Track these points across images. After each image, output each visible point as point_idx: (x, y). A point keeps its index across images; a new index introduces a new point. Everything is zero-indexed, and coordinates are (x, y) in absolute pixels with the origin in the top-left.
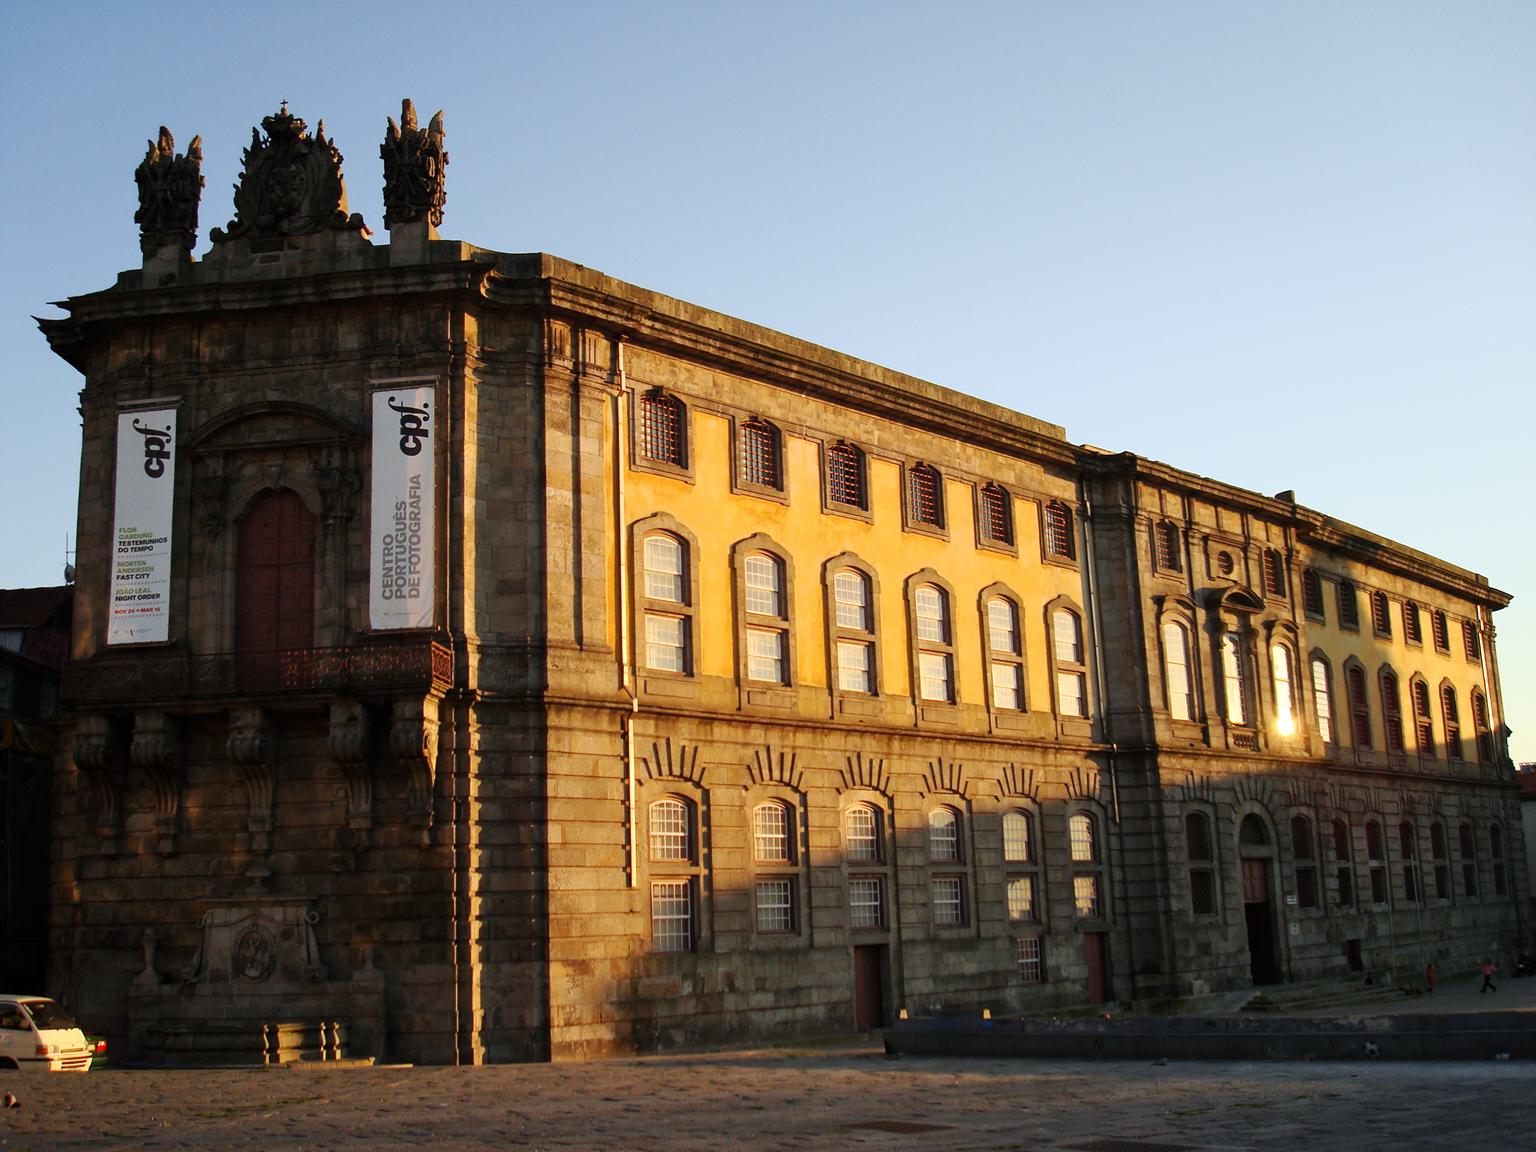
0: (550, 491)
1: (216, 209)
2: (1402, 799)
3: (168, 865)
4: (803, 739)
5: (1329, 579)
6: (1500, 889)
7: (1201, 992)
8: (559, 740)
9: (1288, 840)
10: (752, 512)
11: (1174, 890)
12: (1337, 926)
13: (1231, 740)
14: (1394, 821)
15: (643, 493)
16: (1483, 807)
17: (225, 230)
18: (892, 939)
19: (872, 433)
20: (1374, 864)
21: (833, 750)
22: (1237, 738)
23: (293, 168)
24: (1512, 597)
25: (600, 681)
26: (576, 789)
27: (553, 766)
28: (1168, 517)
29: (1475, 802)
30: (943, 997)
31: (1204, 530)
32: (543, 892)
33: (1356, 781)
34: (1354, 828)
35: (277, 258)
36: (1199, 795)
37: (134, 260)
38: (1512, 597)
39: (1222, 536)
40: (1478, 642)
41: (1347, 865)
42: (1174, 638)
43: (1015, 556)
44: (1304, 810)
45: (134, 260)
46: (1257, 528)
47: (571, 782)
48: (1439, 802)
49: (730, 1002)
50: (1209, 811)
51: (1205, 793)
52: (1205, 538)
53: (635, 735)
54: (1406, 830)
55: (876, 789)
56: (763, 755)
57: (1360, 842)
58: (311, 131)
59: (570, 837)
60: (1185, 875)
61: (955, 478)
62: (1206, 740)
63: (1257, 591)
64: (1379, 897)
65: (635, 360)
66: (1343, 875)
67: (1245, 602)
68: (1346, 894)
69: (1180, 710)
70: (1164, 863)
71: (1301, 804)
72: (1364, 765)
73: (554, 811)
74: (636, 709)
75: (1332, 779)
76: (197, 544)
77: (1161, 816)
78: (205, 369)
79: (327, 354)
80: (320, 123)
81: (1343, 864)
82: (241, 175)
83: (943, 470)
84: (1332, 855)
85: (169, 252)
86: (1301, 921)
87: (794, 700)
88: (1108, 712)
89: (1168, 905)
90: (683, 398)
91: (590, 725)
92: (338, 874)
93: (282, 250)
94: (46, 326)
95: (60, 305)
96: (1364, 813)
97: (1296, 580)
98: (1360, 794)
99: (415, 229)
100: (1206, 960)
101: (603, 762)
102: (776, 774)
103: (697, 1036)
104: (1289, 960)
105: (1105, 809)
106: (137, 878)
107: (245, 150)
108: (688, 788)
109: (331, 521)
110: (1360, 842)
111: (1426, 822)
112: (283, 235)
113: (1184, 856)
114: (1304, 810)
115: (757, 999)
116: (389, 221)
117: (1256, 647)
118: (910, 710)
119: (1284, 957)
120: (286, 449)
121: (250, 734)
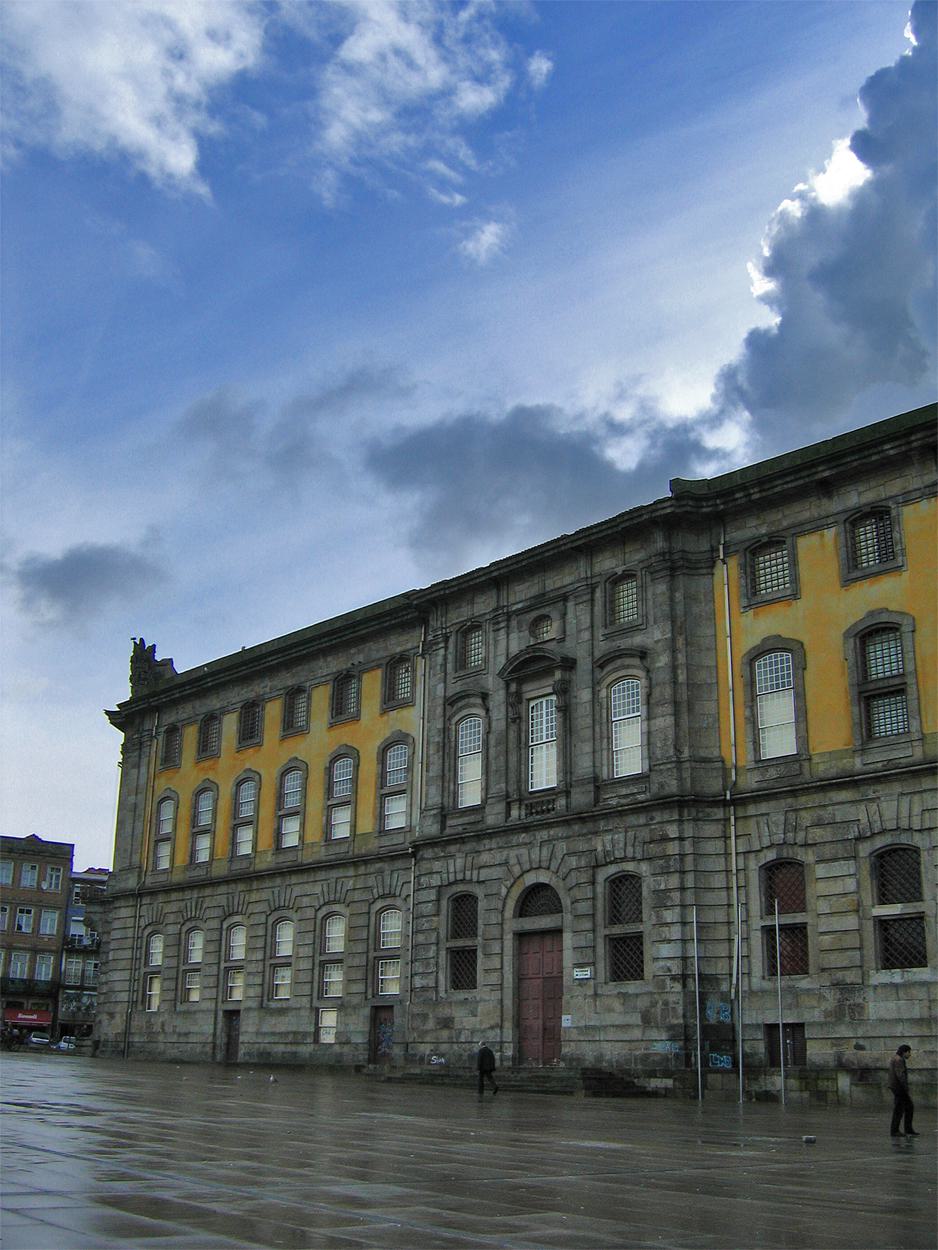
12: (666, 1003)
31: (514, 609)
36: (460, 877)
44: (630, 867)
51: (468, 873)
52: (519, 612)
56: (189, 904)
71: (615, 861)
96: (860, 838)
100: (445, 1034)
102: (193, 913)
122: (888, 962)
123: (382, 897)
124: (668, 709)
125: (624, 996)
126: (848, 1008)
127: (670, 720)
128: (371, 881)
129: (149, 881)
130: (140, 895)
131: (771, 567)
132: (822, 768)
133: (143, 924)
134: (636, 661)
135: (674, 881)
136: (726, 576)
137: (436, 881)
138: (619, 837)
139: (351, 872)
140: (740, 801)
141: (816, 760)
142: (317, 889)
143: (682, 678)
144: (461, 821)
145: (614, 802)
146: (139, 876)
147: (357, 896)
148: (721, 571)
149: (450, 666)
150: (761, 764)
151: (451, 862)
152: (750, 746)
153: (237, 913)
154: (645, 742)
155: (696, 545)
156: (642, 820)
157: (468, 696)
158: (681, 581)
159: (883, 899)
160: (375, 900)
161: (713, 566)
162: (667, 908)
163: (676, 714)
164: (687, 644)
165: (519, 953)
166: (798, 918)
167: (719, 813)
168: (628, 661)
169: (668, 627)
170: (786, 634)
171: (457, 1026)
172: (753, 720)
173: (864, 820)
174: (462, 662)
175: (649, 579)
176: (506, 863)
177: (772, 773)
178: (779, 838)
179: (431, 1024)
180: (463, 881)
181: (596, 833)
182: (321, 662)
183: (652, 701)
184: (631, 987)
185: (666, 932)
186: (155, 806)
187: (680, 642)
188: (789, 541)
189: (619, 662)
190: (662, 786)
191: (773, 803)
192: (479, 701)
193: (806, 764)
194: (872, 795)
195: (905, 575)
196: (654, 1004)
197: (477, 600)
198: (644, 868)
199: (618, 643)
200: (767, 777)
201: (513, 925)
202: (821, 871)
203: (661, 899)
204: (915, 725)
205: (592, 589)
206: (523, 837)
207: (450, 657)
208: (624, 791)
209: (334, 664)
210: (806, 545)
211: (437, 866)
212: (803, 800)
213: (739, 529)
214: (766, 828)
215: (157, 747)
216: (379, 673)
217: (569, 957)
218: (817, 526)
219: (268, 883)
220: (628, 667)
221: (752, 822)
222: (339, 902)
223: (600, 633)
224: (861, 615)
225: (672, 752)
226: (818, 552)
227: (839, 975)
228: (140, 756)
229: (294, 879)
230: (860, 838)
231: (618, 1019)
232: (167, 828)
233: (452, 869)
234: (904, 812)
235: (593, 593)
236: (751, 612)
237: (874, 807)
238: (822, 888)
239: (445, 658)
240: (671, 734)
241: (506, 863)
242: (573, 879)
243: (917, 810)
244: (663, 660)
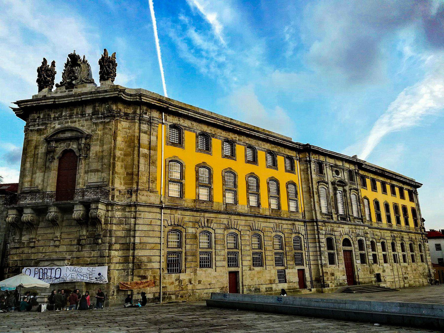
0: (141, 149)
1: (58, 79)
2: (392, 236)
3: (33, 250)
5: (368, 178)
6: (422, 261)
7: (332, 286)
8: (140, 215)
9: (357, 246)
11: (323, 258)
13: (339, 219)
14: (391, 241)
16: (416, 239)
17: (59, 84)
18: (240, 270)
19: (236, 138)
20: (384, 253)
21: (224, 219)
22: (341, 218)
23: (76, 67)
24: (422, 185)
25: (154, 199)
26: (146, 228)
27: (139, 221)
28: (321, 161)
29: (414, 237)
30: (255, 286)
31: (331, 164)
32: (134, 256)
33: (378, 231)
34: (377, 243)
35: (72, 91)
37: (36, 93)
38: (422, 185)
39: (336, 166)
40: (413, 196)
41: (376, 253)
42: (323, 192)
43: (277, 169)
44: (362, 238)
45: (36, 93)
46: (347, 165)
47: (143, 226)
48: (403, 237)
49: (190, 287)
50: (333, 237)
52: (332, 166)
53: (164, 213)
54: (393, 245)
55: (236, 229)
56: (202, 219)
57: (379, 246)
58: (82, 58)
59: (142, 241)
60: (326, 253)
61: (259, 150)
62: (332, 218)
63: (347, 181)
64: (386, 262)
65: (168, 117)
66: (374, 256)
67: (342, 183)
68: (375, 260)
69: (324, 210)
70: (320, 251)
72: (380, 227)
73: (137, 234)
74: (164, 207)
75: (370, 230)
76: (48, 164)
77: (319, 238)
78: (52, 119)
79: (83, 115)
80: (84, 57)
81: (374, 253)
82: (64, 70)
83: (257, 148)
84: (370, 250)
85: (45, 90)
87: (212, 205)
88: (304, 211)
89: (321, 262)
90: (182, 127)
92: (77, 251)
93: (73, 88)
94: (14, 110)
95: (15, 103)
96: (380, 239)
97: (358, 178)
98: (379, 234)
99: (109, 82)
100: (333, 277)
101: (153, 220)
102: (206, 225)
103: (179, 297)
104: (358, 278)
105: (303, 236)
106: (25, 253)
107: (65, 64)
108: (179, 228)
109: (81, 157)
110: (379, 246)
111: (400, 242)
112: (74, 85)
113: (326, 248)
114: (362, 238)
115: (199, 286)
116: (100, 80)
117: (346, 194)
118: (246, 209)
119: (357, 277)
120: (71, 139)
121: (53, 213)
123: (295, 233)
144: (326, 217)
153: (232, 228)
176: (340, 231)
196: (371, 270)
211: (324, 228)
229: (261, 220)
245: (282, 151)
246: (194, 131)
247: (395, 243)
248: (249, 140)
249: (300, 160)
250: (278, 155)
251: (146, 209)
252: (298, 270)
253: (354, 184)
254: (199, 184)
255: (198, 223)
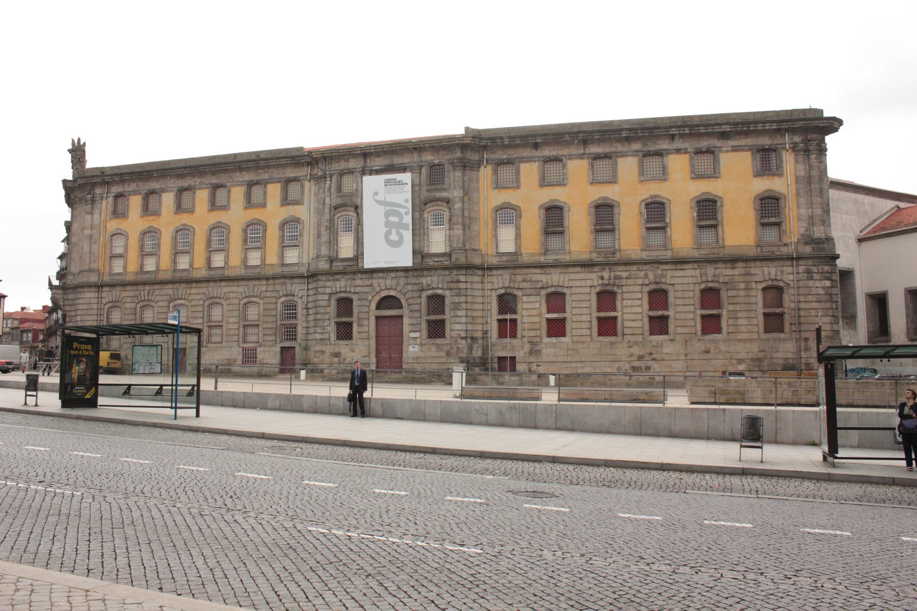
4: (157, 287)
10: (147, 220)
12: (458, 348)
15: (113, 225)
26: (85, 307)
36: (343, 290)
44: (439, 292)
56: (142, 293)
71: (433, 289)
83: (228, 184)
86: (421, 345)
91: (89, 290)
96: (542, 288)
98: (540, 277)
100: (336, 359)
101: (92, 300)
122: (549, 335)
124: (460, 227)
125: (438, 345)
126: (534, 351)
127: (461, 232)
128: (278, 288)
129: (107, 279)
130: (102, 286)
131: (506, 172)
132: (526, 259)
133: (104, 301)
134: (445, 204)
135: (463, 299)
136: (486, 173)
137: (328, 291)
138: (435, 279)
139: (264, 282)
140: (490, 268)
141: (523, 255)
142: (241, 289)
143: (466, 214)
144: (342, 264)
145: (432, 263)
146: (99, 275)
147: (268, 294)
148: (482, 169)
149: (333, 190)
150: (499, 254)
151: (338, 283)
152: (495, 246)
153: (181, 299)
154: (447, 239)
155: (475, 157)
156: (447, 272)
157: (346, 206)
158: (468, 172)
159: (549, 311)
160: (280, 297)
161: (479, 168)
162: (459, 310)
163: (464, 229)
164: (469, 200)
165: (377, 325)
166: (514, 316)
167: (480, 272)
168: (439, 203)
169: (461, 191)
170: (513, 202)
171: (343, 356)
172: (495, 236)
173: (544, 281)
174: (339, 189)
175: (451, 168)
176: (371, 285)
177: (504, 258)
178: (507, 284)
179: (327, 356)
180: (345, 292)
181: (422, 276)
182: (238, 174)
183: (452, 222)
184: (439, 341)
185: (458, 319)
186: (108, 237)
187: (466, 198)
188: (516, 164)
189: (435, 203)
190: (457, 259)
191: (504, 271)
192: (353, 209)
193: (520, 257)
194: (548, 272)
195: (567, 188)
196: (452, 348)
197: (350, 160)
198: (447, 293)
199: (434, 194)
200: (502, 259)
201: (374, 312)
202: (525, 299)
203: (456, 307)
204: (567, 247)
205: (421, 167)
206: (380, 275)
207: (333, 185)
208: (437, 259)
209: (248, 177)
210: (524, 167)
211: (328, 284)
212: (518, 271)
213: (493, 153)
214: (500, 281)
215: (106, 205)
216: (279, 185)
217: (406, 328)
218: (530, 160)
219: (203, 285)
220: (440, 206)
221: (495, 277)
222: (256, 297)
223: (424, 188)
224: (547, 200)
225: (461, 245)
226: (529, 171)
227: (531, 339)
228: (92, 208)
229: (223, 284)
230: (542, 288)
231: (435, 354)
232: (119, 250)
233: (338, 286)
234: (562, 279)
235: (421, 169)
236: (496, 191)
237: (549, 276)
238: (525, 306)
239: (330, 186)
240: (461, 237)
241: (371, 285)
242: (409, 295)
243: (566, 279)
244: (458, 206)
245: (278, 174)
246: (139, 194)
247: (620, 291)
248: (217, 178)
249: (313, 178)
250: (268, 183)
251: (86, 290)
252: (282, 348)
253: (445, 190)
254: (143, 254)
255: (137, 297)
